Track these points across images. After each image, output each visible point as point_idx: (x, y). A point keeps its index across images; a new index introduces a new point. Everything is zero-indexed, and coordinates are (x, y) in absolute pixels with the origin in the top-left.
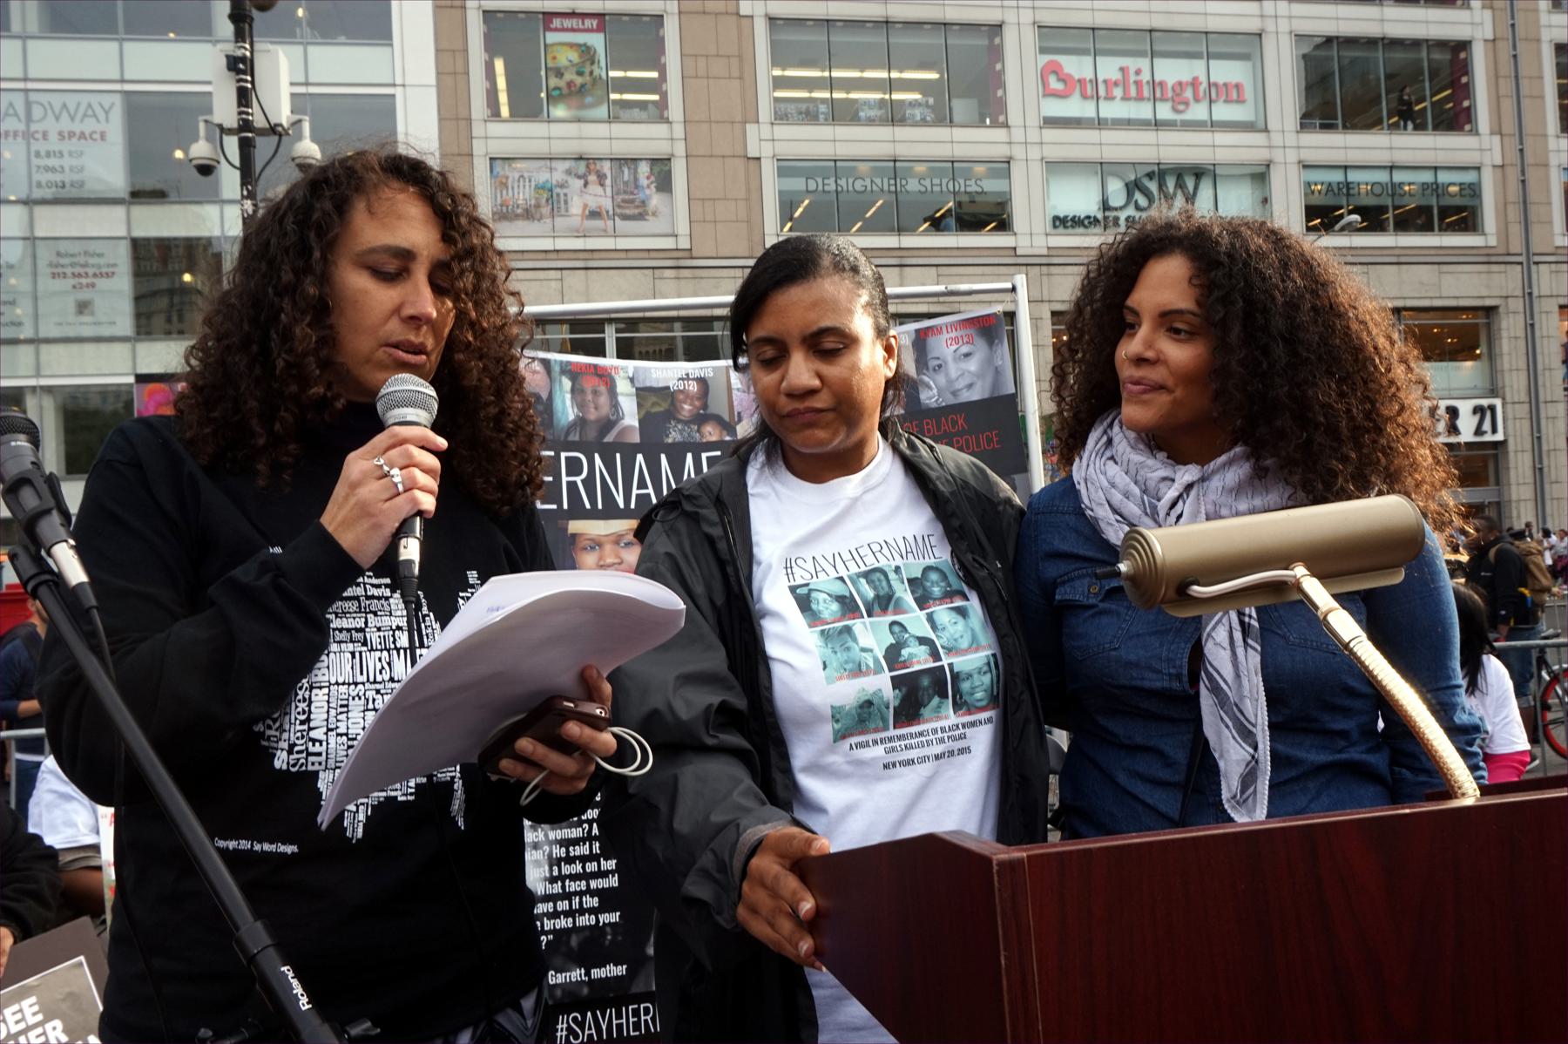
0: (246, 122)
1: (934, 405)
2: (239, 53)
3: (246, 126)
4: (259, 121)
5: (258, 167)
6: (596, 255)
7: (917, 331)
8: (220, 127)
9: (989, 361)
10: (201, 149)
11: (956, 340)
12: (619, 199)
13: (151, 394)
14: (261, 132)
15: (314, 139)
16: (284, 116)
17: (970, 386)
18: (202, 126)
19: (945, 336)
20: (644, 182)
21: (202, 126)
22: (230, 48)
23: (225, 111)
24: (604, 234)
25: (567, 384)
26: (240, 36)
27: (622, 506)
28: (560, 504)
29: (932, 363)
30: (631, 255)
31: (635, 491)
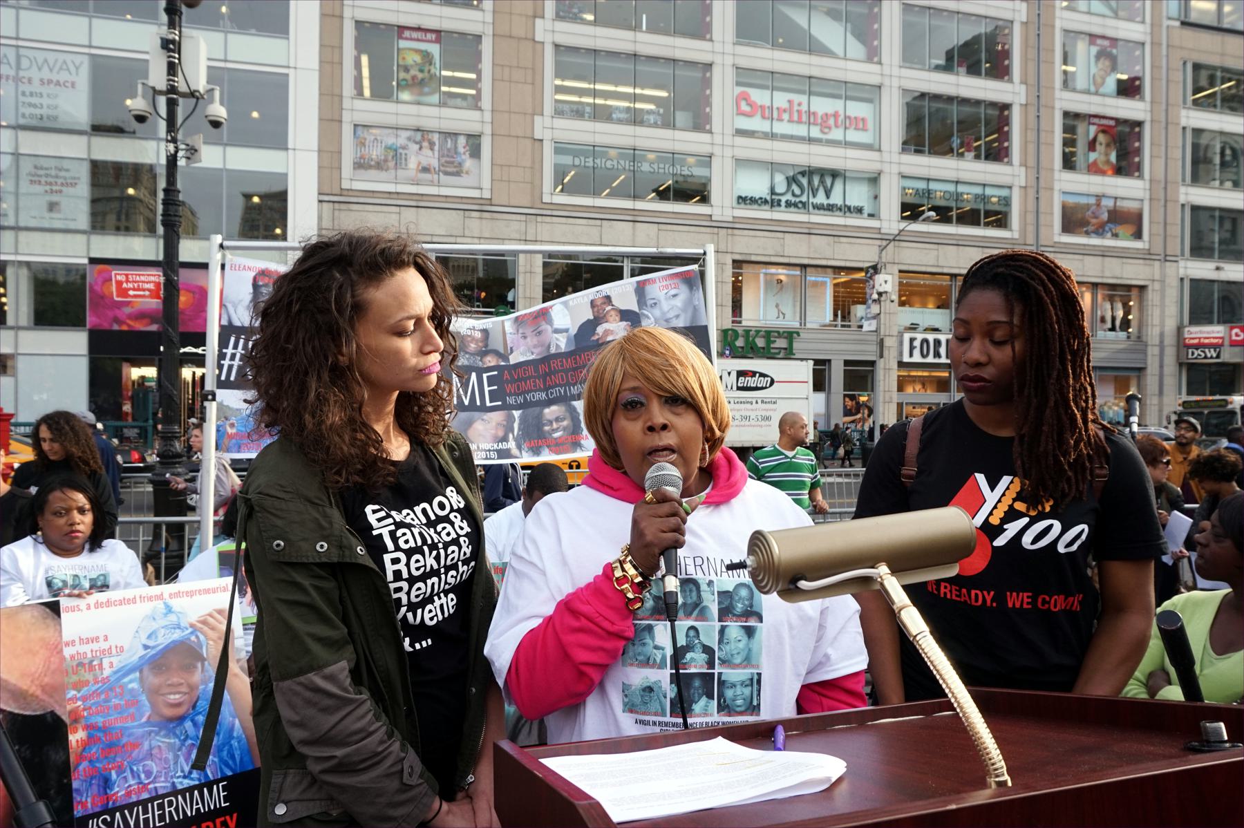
0: (173, 86)
2: (171, 37)
3: (172, 89)
4: (182, 87)
5: (180, 120)
8: (153, 88)
10: (137, 104)
12: (443, 160)
13: (100, 272)
14: (184, 95)
15: (222, 103)
16: (201, 83)
18: (140, 87)
19: (658, 284)
20: (461, 150)
21: (140, 87)
22: (164, 31)
23: (158, 77)
24: (431, 184)
26: (172, 25)
29: (650, 302)
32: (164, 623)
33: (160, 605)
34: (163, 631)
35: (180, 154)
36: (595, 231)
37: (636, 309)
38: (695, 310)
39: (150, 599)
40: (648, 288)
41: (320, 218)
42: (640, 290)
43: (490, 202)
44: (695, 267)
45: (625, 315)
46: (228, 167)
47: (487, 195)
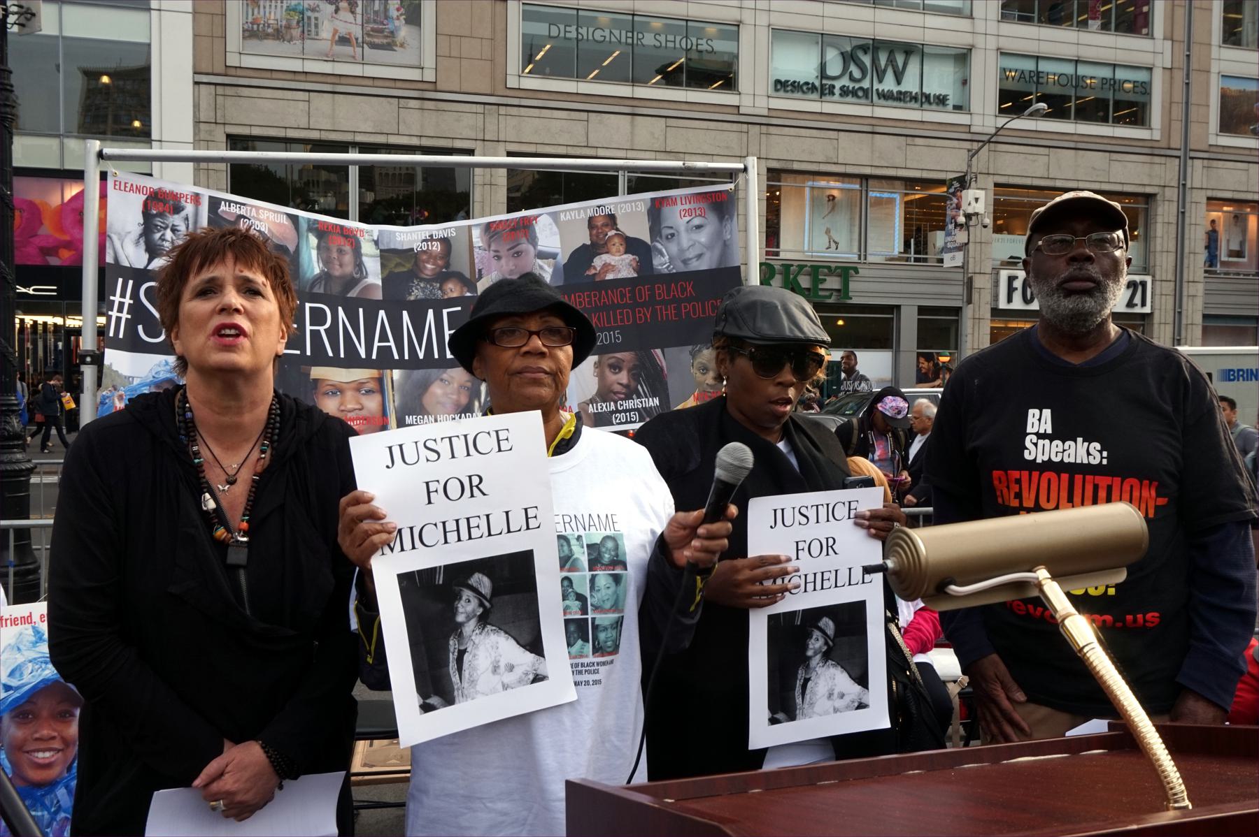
1: (666, 271)
6: (343, 80)
7: (653, 200)
9: (718, 234)
12: (369, 27)
17: (699, 256)
19: (679, 207)
20: (393, 13)
24: (353, 60)
27: (363, 356)
28: (303, 350)
29: (666, 232)
30: (378, 83)
31: (376, 344)
32: (32, 655)
33: (27, 630)
34: (30, 665)
35: (12, 19)
36: (579, 128)
37: (646, 237)
39: (14, 621)
40: (666, 210)
41: (196, 107)
42: (655, 212)
45: (632, 245)
46: (68, 33)
47: (429, 76)
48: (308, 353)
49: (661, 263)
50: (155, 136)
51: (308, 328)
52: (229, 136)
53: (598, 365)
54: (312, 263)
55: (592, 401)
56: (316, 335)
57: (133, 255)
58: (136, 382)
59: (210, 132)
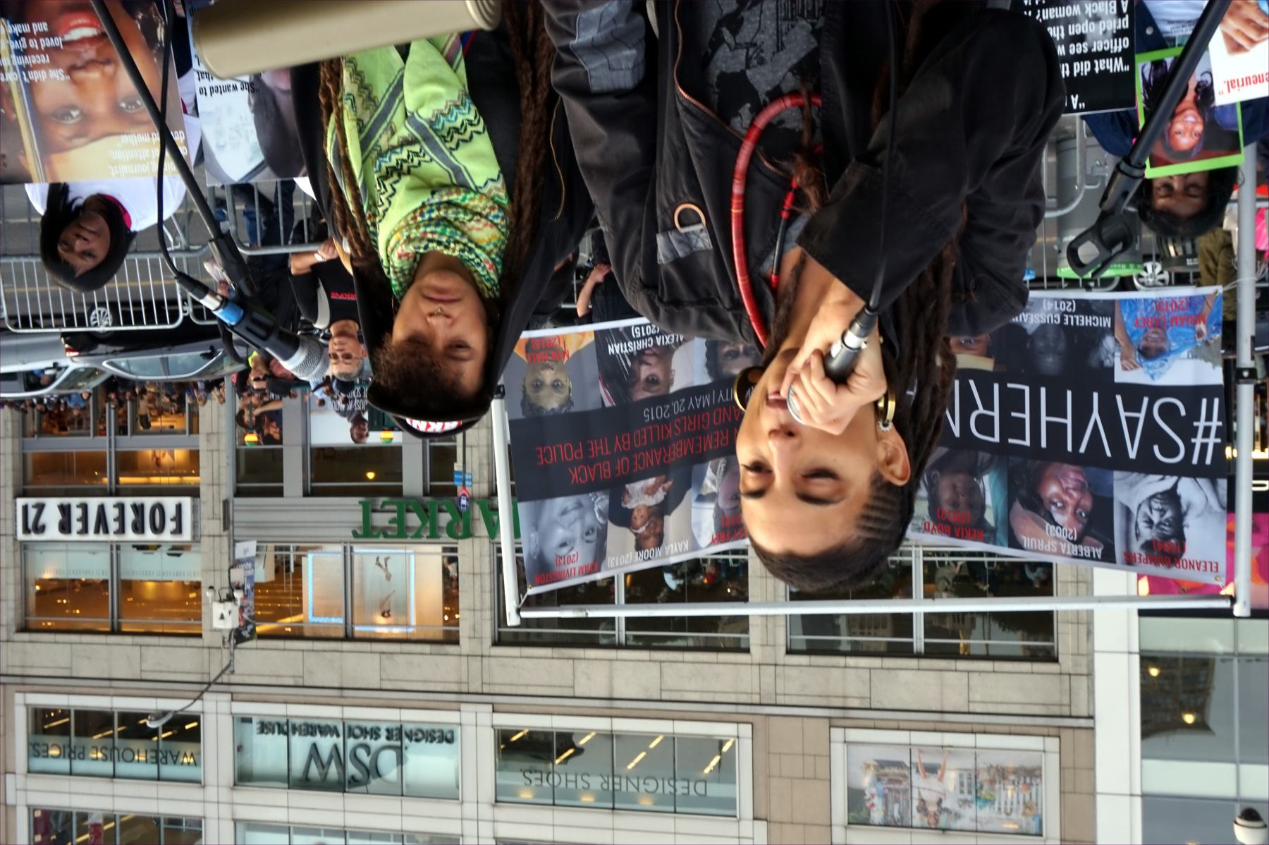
6: (931, 726)
11: (570, 560)
12: (905, 785)
20: (878, 801)
24: (922, 748)
25: (989, 517)
30: (894, 724)
36: (670, 682)
38: (535, 525)
41: (1091, 691)
43: (832, 723)
44: (531, 591)
46: (1229, 768)
47: (837, 734)
48: (996, 386)
49: (601, 502)
50: (1136, 659)
51: (996, 414)
52: (1055, 660)
53: (669, 382)
54: (990, 487)
55: (680, 343)
56: (988, 405)
57: (1189, 489)
58: (1185, 354)
59: (1076, 664)
